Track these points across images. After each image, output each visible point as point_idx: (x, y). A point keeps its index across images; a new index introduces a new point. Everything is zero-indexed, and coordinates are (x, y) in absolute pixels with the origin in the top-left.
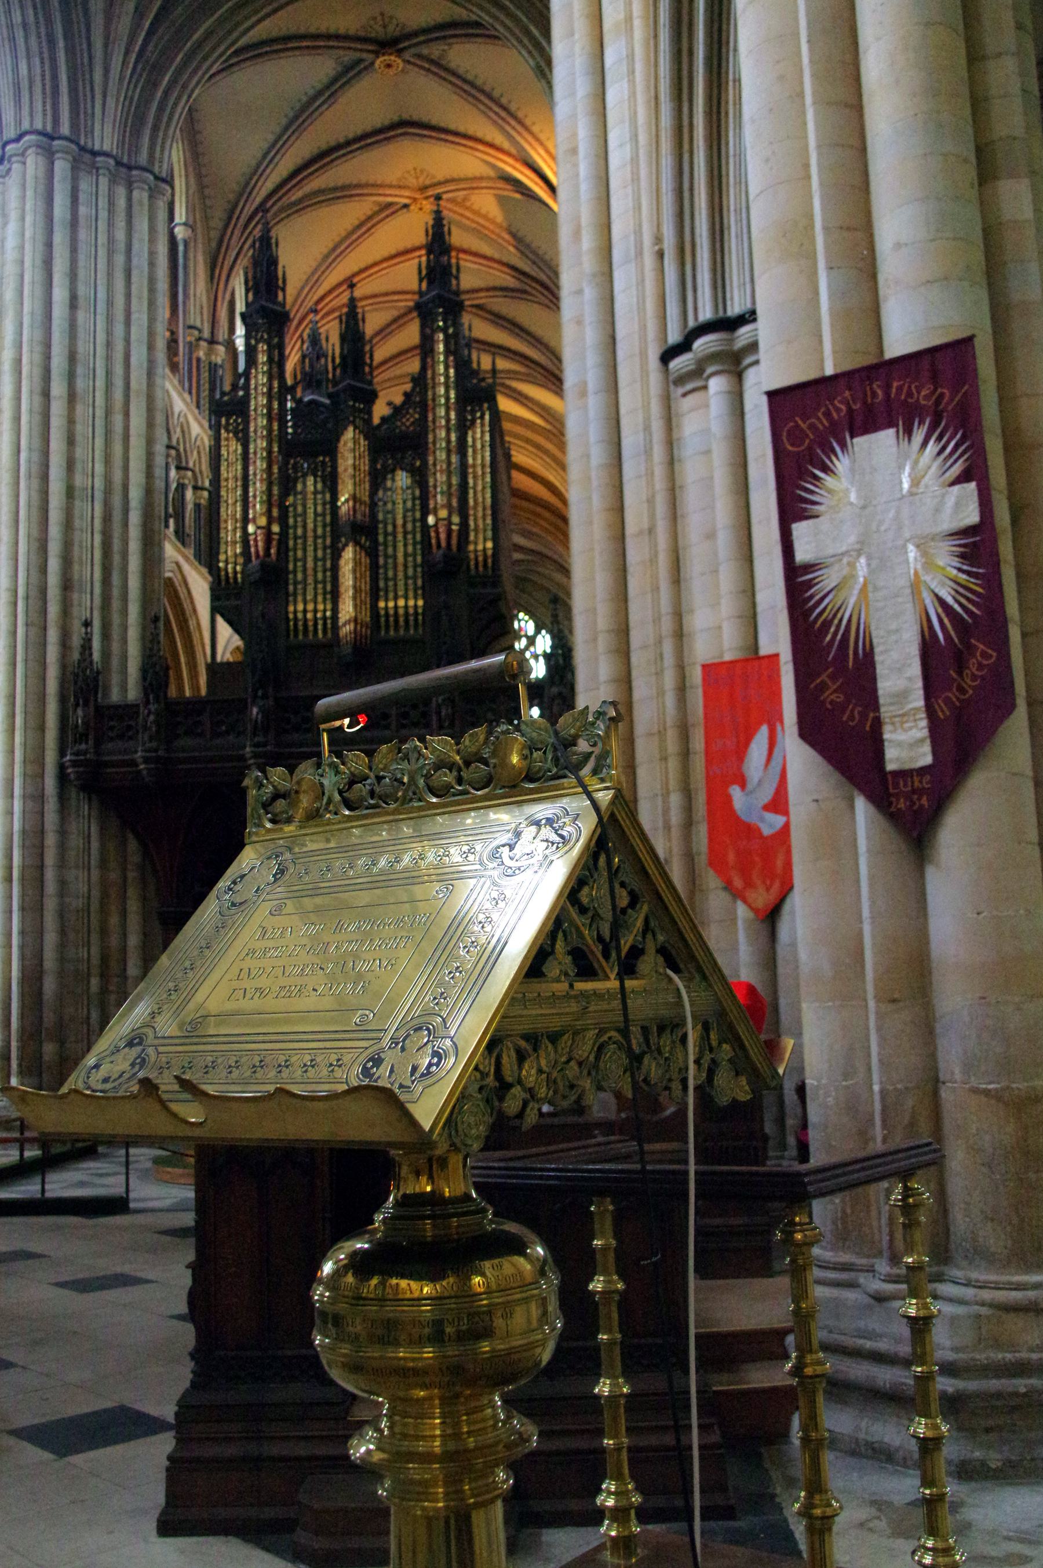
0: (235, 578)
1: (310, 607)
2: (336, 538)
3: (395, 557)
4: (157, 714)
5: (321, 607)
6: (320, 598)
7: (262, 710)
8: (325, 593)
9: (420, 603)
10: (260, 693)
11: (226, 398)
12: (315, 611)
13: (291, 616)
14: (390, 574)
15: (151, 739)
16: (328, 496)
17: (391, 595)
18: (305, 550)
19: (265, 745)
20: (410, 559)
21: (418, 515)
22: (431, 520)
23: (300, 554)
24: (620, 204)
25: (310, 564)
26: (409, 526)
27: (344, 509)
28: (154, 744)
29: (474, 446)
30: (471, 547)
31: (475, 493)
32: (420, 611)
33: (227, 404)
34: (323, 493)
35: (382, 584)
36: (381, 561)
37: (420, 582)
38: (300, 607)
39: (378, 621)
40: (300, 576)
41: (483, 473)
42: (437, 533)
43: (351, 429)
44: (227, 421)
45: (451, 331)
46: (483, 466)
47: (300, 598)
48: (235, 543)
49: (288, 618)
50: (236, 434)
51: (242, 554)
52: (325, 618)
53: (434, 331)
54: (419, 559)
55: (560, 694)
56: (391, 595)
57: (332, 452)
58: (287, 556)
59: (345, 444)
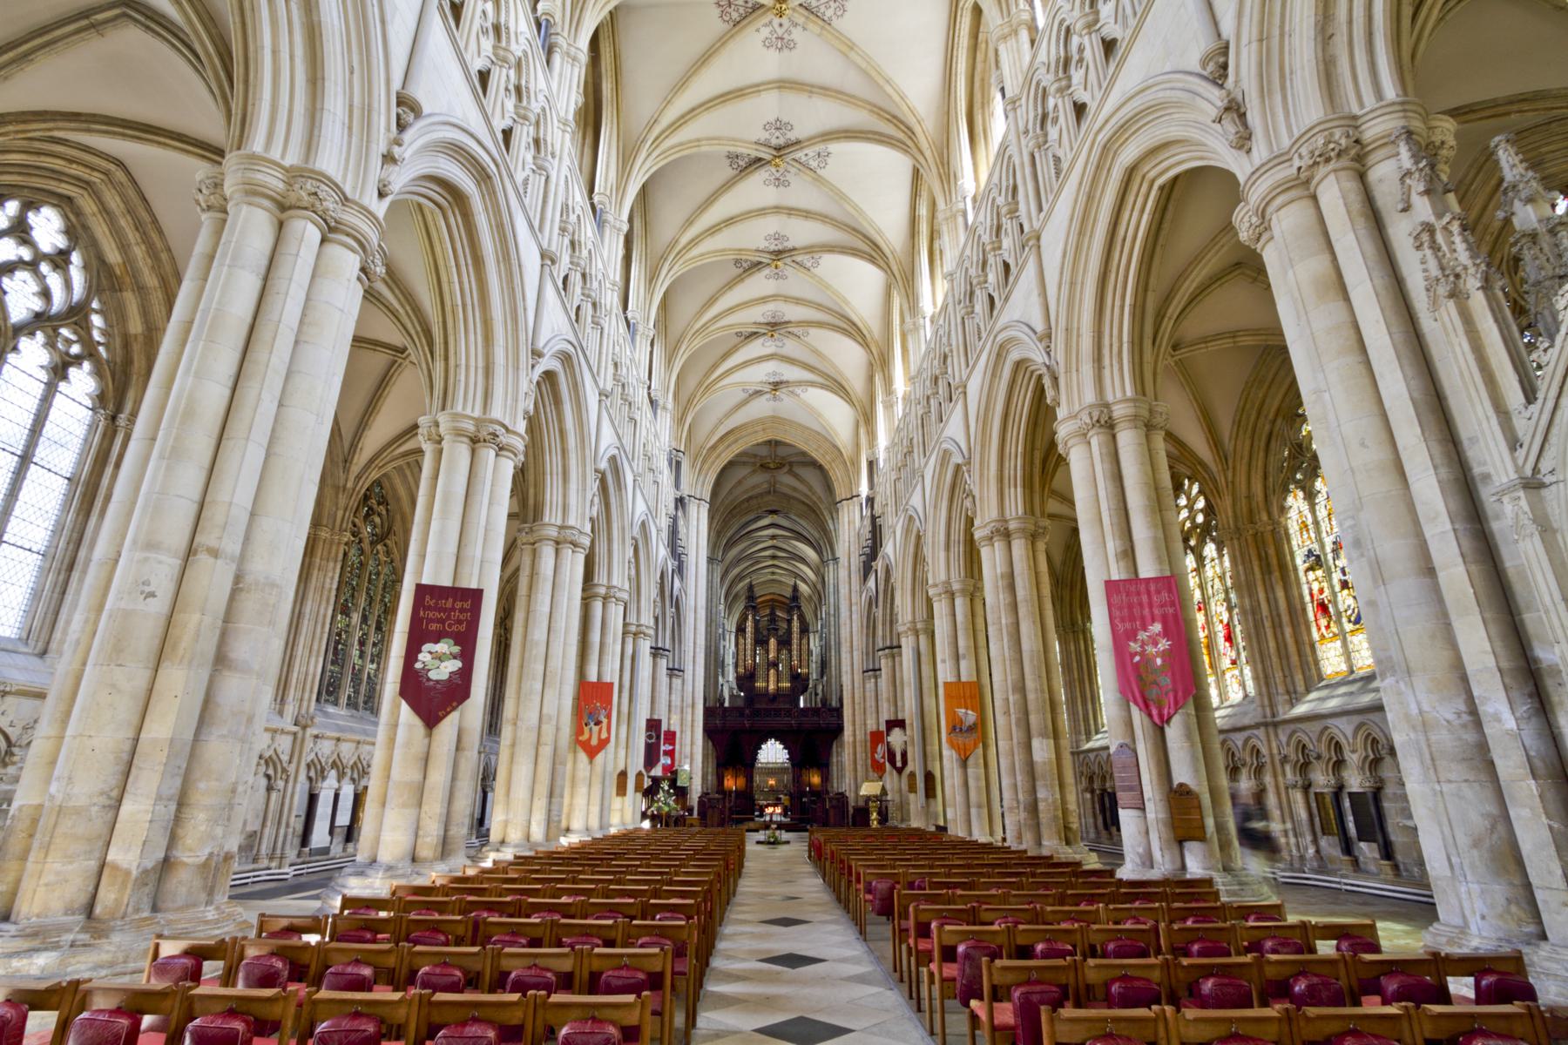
24: (855, 638)
57: (767, 642)
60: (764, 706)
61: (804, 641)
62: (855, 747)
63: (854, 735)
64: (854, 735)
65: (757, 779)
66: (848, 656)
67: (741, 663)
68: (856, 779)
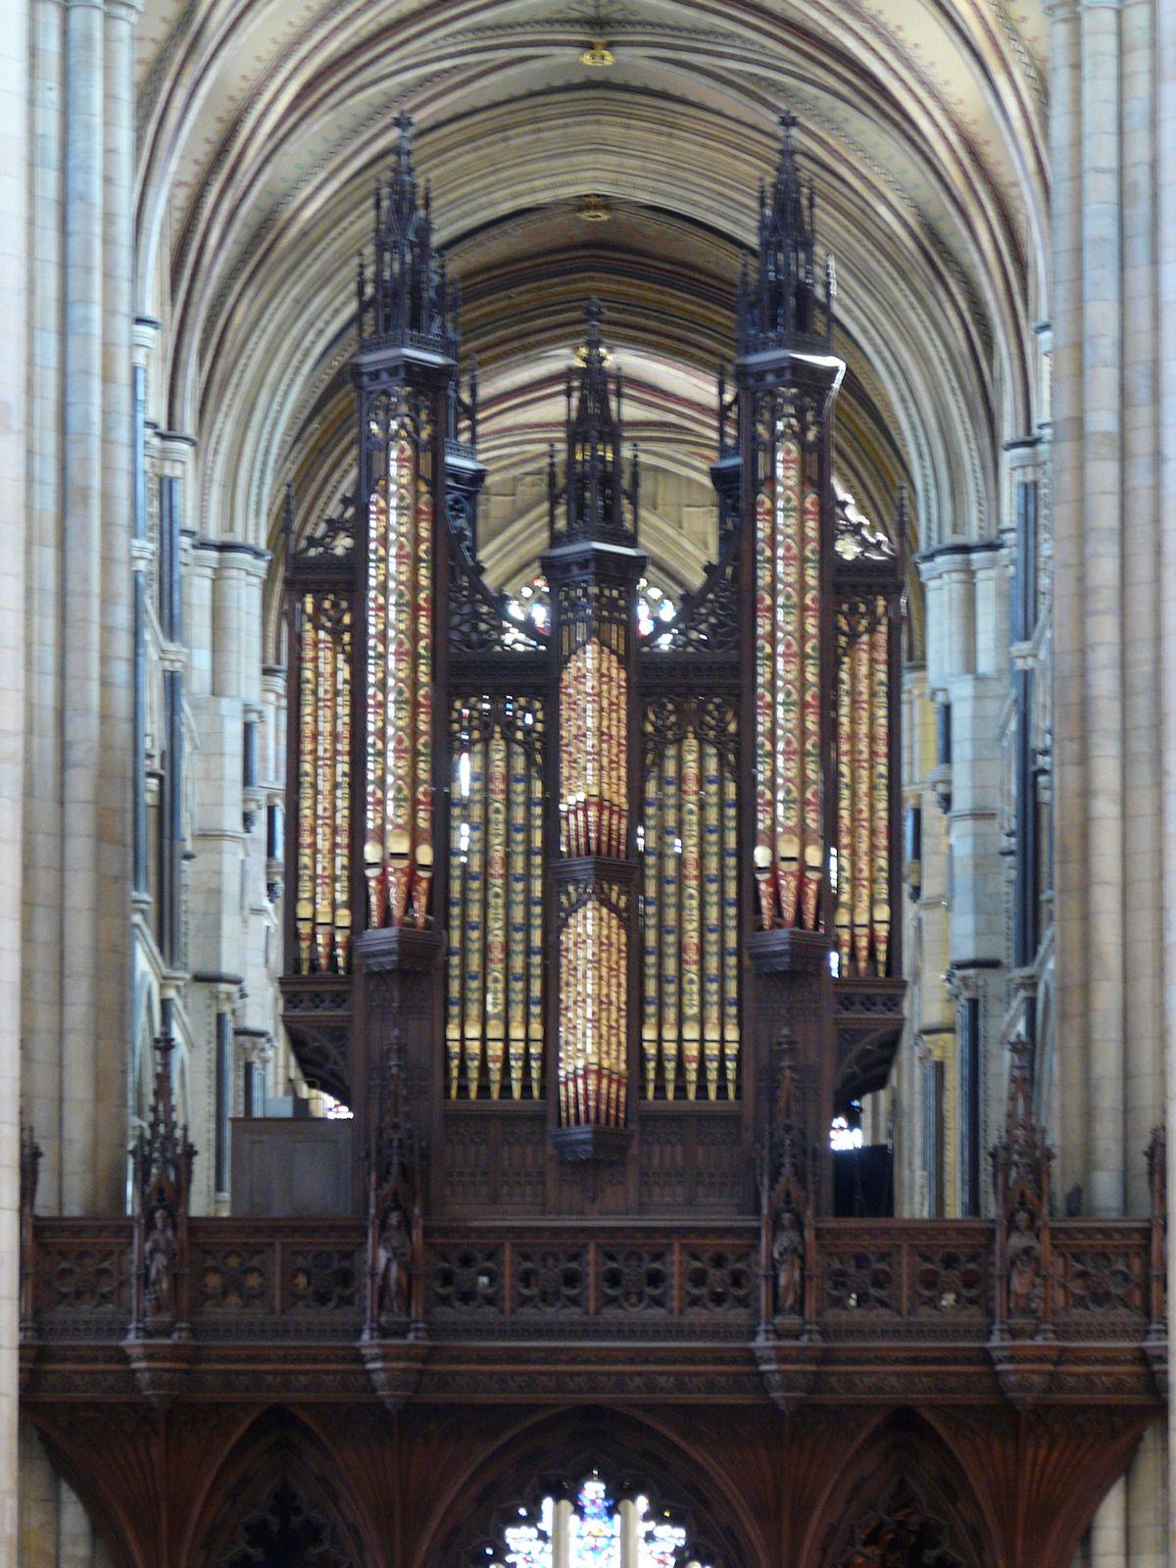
0: (332, 958)
1: (495, 1030)
2: (556, 881)
3: (680, 930)
4: (172, 1255)
5: (517, 1032)
6: (517, 1012)
7: (395, 1254)
8: (527, 1002)
9: (732, 1034)
10: (394, 1218)
11: (312, 552)
12: (507, 1040)
13: (455, 1048)
15: (158, 1308)
16: (538, 787)
17: (671, 1014)
18: (485, 905)
19: (402, 1333)
20: (713, 937)
21: (731, 840)
22: (761, 855)
23: (475, 913)
25: (497, 937)
26: (713, 865)
27: (574, 824)
28: (166, 1318)
29: (853, 693)
30: (843, 918)
31: (854, 795)
32: (731, 1050)
33: (313, 565)
34: (527, 780)
36: (651, 938)
38: (473, 1031)
39: (643, 1070)
40: (475, 962)
41: (873, 754)
42: (774, 883)
43: (591, 649)
44: (318, 607)
45: (811, 436)
46: (872, 739)
47: (474, 1010)
48: (334, 879)
49: (446, 1049)
50: (336, 633)
51: (350, 904)
52: (527, 1057)
55: (1027, 1251)
56: (671, 1014)
58: (447, 917)
59: (580, 678)
61: (863, 669)
67: (324, 854)
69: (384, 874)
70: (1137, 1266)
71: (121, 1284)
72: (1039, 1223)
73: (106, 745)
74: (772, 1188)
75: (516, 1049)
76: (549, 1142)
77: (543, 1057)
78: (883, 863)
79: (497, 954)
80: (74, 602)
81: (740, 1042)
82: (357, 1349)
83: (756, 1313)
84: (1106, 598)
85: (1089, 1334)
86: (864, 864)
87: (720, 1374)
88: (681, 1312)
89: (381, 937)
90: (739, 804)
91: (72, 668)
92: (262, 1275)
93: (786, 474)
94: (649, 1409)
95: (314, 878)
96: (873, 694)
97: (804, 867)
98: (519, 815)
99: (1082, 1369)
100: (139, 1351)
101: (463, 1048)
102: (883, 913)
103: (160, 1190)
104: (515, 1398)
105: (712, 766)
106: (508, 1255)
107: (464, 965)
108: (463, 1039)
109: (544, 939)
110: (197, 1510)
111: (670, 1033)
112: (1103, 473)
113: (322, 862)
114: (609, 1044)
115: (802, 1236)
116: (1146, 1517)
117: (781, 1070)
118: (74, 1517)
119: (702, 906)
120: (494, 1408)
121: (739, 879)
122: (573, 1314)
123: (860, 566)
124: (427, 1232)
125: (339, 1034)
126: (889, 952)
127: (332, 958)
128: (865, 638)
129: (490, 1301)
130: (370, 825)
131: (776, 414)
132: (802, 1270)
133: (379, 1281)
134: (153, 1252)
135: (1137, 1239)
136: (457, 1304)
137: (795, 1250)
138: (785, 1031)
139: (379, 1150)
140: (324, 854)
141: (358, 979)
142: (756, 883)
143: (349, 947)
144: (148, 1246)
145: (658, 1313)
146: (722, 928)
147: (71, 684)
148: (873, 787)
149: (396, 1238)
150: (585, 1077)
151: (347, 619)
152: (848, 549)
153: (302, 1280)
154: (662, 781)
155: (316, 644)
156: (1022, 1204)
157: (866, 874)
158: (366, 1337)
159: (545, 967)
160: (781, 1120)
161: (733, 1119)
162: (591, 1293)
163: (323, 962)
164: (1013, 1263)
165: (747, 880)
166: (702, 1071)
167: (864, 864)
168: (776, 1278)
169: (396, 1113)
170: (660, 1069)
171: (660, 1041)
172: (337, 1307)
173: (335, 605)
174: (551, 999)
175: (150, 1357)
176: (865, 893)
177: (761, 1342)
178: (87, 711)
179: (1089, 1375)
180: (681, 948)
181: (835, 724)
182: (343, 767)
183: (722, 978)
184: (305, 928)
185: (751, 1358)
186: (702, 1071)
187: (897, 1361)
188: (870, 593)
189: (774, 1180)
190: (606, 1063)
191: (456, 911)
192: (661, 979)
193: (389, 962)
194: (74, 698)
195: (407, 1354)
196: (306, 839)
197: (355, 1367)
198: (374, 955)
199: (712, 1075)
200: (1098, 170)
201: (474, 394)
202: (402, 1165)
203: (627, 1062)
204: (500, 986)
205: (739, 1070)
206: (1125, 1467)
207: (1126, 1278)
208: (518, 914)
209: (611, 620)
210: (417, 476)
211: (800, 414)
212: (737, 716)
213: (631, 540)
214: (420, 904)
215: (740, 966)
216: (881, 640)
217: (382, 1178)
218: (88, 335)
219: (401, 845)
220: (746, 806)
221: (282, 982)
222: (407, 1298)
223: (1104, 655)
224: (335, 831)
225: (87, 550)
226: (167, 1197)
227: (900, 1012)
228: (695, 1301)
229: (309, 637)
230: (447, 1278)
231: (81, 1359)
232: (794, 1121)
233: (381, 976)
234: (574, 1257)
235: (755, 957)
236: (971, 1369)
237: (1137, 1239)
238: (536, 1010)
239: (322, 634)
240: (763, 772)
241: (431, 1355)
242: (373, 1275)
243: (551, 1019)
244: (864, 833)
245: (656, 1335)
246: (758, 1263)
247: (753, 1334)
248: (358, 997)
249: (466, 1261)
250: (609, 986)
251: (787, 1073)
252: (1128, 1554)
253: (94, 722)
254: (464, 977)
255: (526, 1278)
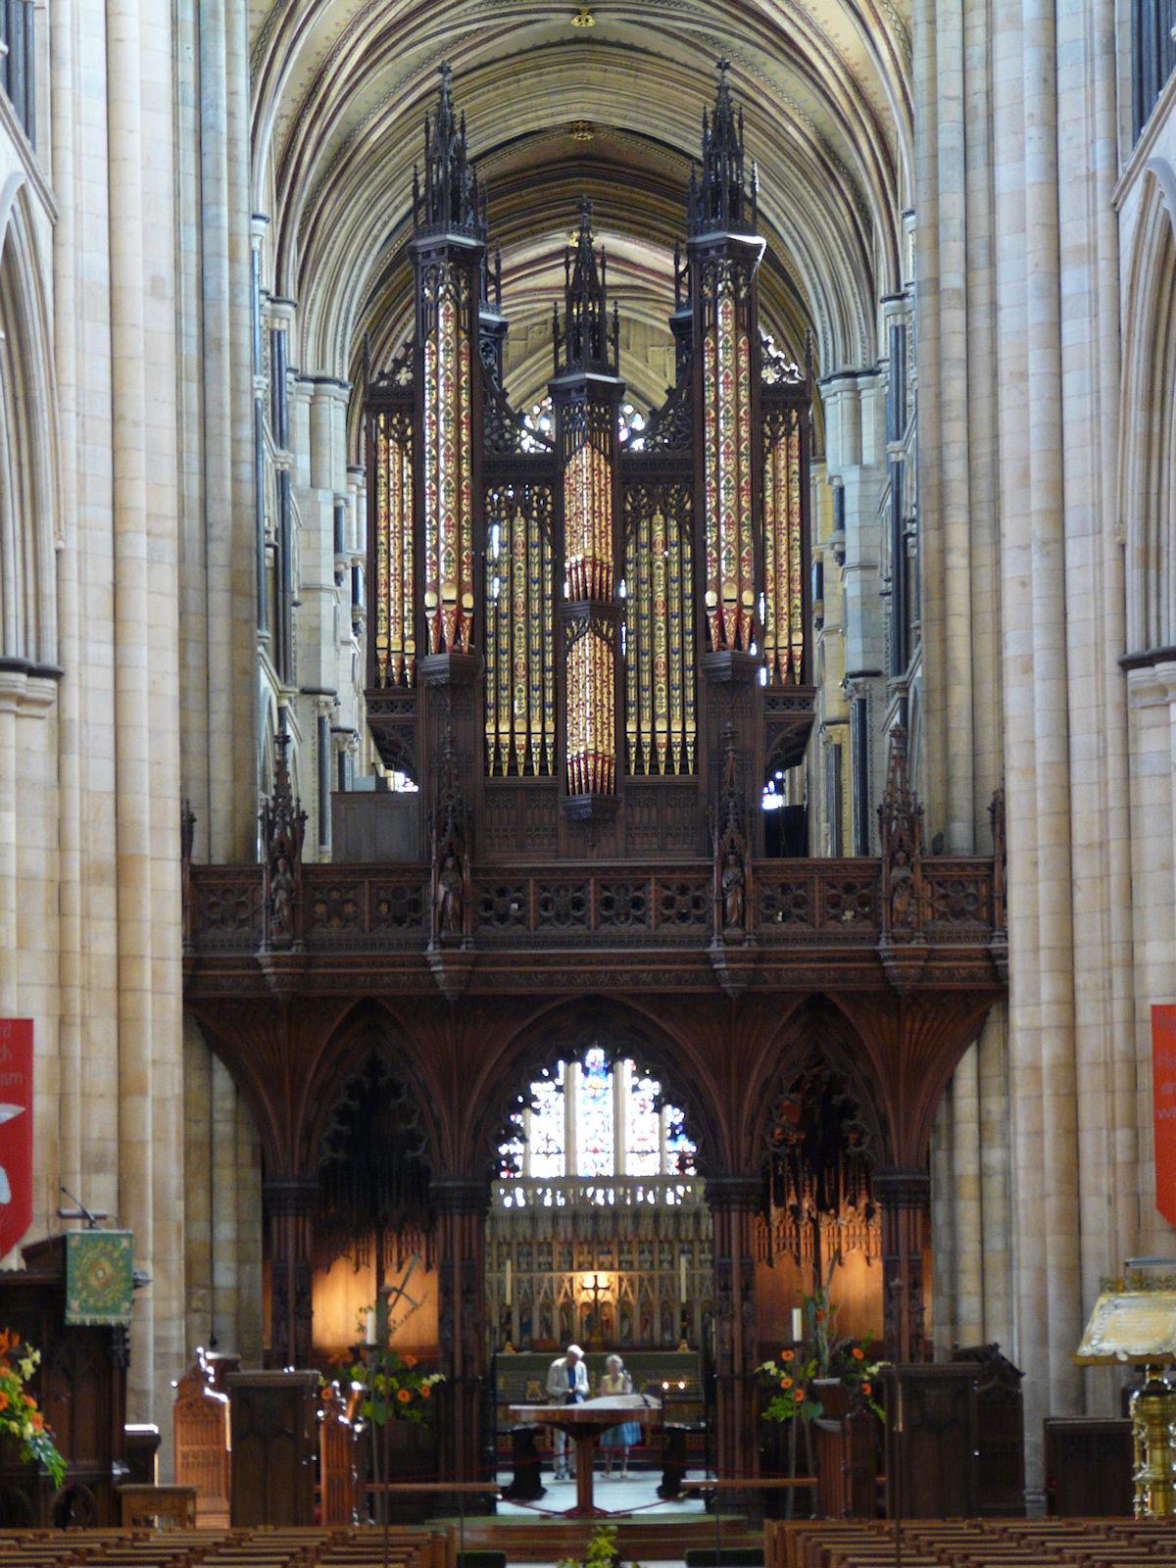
0: (402, 676)
1: (520, 726)
3: (652, 653)
4: (290, 891)
5: (536, 728)
6: (536, 713)
7: (451, 888)
8: (543, 706)
9: (691, 727)
10: (449, 863)
11: (383, 384)
12: (529, 733)
13: (492, 739)
14: (646, 679)
15: (281, 929)
16: (548, 551)
17: (647, 713)
21: (688, 587)
22: (710, 598)
23: (504, 642)
25: (520, 659)
26: (675, 605)
28: (287, 936)
29: (775, 479)
31: (776, 553)
32: (690, 739)
33: (384, 392)
35: (632, 694)
37: (690, 694)
38: (504, 727)
39: (627, 754)
40: (505, 677)
41: (789, 524)
42: (720, 617)
44: (388, 422)
45: (742, 294)
46: (789, 513)
47: (505, 712)
48: (403, 619)
49: (485, 740)
50: (402, 442)
51: (415, 637)
53: (717, 296)
54: (689, 659)
55: (905, 880)
56: (647, 713)
58: (485, 645)
60: (537, 860)
61: (782, 462)
62: (1071, 1097)
63: (1070, 1029)
64: (1070, 1029)
65: (506, 1279)
66: (1038, 564)
67: (395, 601)
68: (1074, 1272)
69: (439, 612)
70: (983, 889)
71: (255, 912)
72: (913, 859)
73: (237, 525)
74: (721, 837)
75: (536, 739)
76: (561, 807)
77: (555, 745)
78: (798, 602)
79: (521, 671)
80: (211, 422)
81: (696, 732)
82: (424, 957)
83: (711, 927)
84: (957, 409)
85: (949, 940)
86: (784, 603)
87: (685, 971)
88: (657, 927)
89: (437, 661)
90: (693, 561)
91: (211, 470)
92: (355, 904)
93: (725, 323)
94: (634, 996)
95: (388, 619)
96: (789, 481)
97: (741, 607)
98: (535, 571)
99: (945, 964)
100: (268, 961)
101: (497, 739)
102: (798, 638)
103: (282, 845)
104: (540, 990)
105: (674, 534)
106: (531, 887)
107: (497, 679)
108: (497, 733)
109: (555, 660)
110: (310, 1075)
111: (646, 727)
112: (954, 319)
113: (394, 607)
114: (602, 735)
115: (743, 871)
116: (992, 1070)
117: (726, 753)
118: (223, 1080)
119: (668, 636)
120: (522, 998)
121: (694, 615)
122: (580, 929)
123: (779, 387)
124: (474, 872)
125: (408, 730)
126: (803, 666)
127: (402, 676)
128: (783, 440)
129: (519, 921)
130: (428, 580)
131: (717, 279)
132: (743, 896)
133: (439, 908)
134: (276, 889)
135: (983, 871)
136: (496, 923)
137: (738, 882)
138: (729, 725)
139: (438, 814)
140: (395, 601)
141: (422, 691)
142: (707, 618)
143: (415, 667)
144: (273, 885)
145: (641, 928)
146: (682, 651)
147: (211, 481)
148: (790, 548)
149: (451, 877)
150: (585, 759)
151: (409, 432)
152: (770, 376)
153: (384, 908)
154: (638, 546)
155: (387, 450)
156: (901, 846)
157: (785, 610)
158: (431, 948)
159: (555, 680)
160: (726, 789)
161: (694, 788)
162: (592, 914)
163: (396, 679)
164: (895, 889)
165: (700, 615)
166: (669, 754)
167: (784, 603)
168: (724, 903)
169: (450, 787)
170: (639, 753)
171: (639, 732)
172: (410, 926)
173: (401, 422)
174: (560, 702)
175: (276, 965)
176: (785, 624)
177: (714, 947)
178: (222, 500)
179: (949, 969)
180: (653, 666)
181: (763, 502)
182: (408, 538)
183: (683, 687)
184: (382, 655)
185: (707, 959)
186: (669, 754)
187: (811, 961)
188: (786, 407)
189: (722, 832)
190: (600, 749)
191: (491, 641)
192: (639, 687)
193: (443, 678)
194: (213, 491)
195: (460, 960)
196: (382, 590)
197: (425, 969)
198: (433, 673)
199: (677, 757)
200: (949, 98)
201: (498, 267)
202: (455, 824)
203: (615, 747)
204: (523, 695)
205: (695, 752)
206: (977, 1034)
207: (976, 899)
208: (536, 643)
209: (600, 430)
210: (458, 327)
211: (734, 279)
212: (691, 497)
213: (614, 372)
214: (465, 635)
215: (695, 677)
216: (795, 440)
217: (441, 834)
218: (219, 227)
219: (450, 594)
220: (699, 563)
221: (366, 693)
222: (460, 919)
223: (956, 450)
224: (403, 585)
225: (220, 384)
226: (286, 850)
227: (811, 710)
228: (667, 919)
229: (382, 444)
230: (488, 905)
231: (225, 967)
232: (736, 789)
233: (438, 688)
234: (579, 889)
235: (707, 672)
236: (865, 965)
237: (983, 871)
238: (549, 711)
239: (391, 442)
240: (710, 538)
241: (477, 961)
242: (435, 904)
243: (560, 717)
244: (785, 581)
245: (639, 943)
246: (711, 891)
247: (709, 943)
248: (422, 703)
249: (502, 892)
250: (602, 693)
251: (731, 754)
252: (980, 1097)
253: (229, 509)
254: (497, 689)
255: (545, 904)
